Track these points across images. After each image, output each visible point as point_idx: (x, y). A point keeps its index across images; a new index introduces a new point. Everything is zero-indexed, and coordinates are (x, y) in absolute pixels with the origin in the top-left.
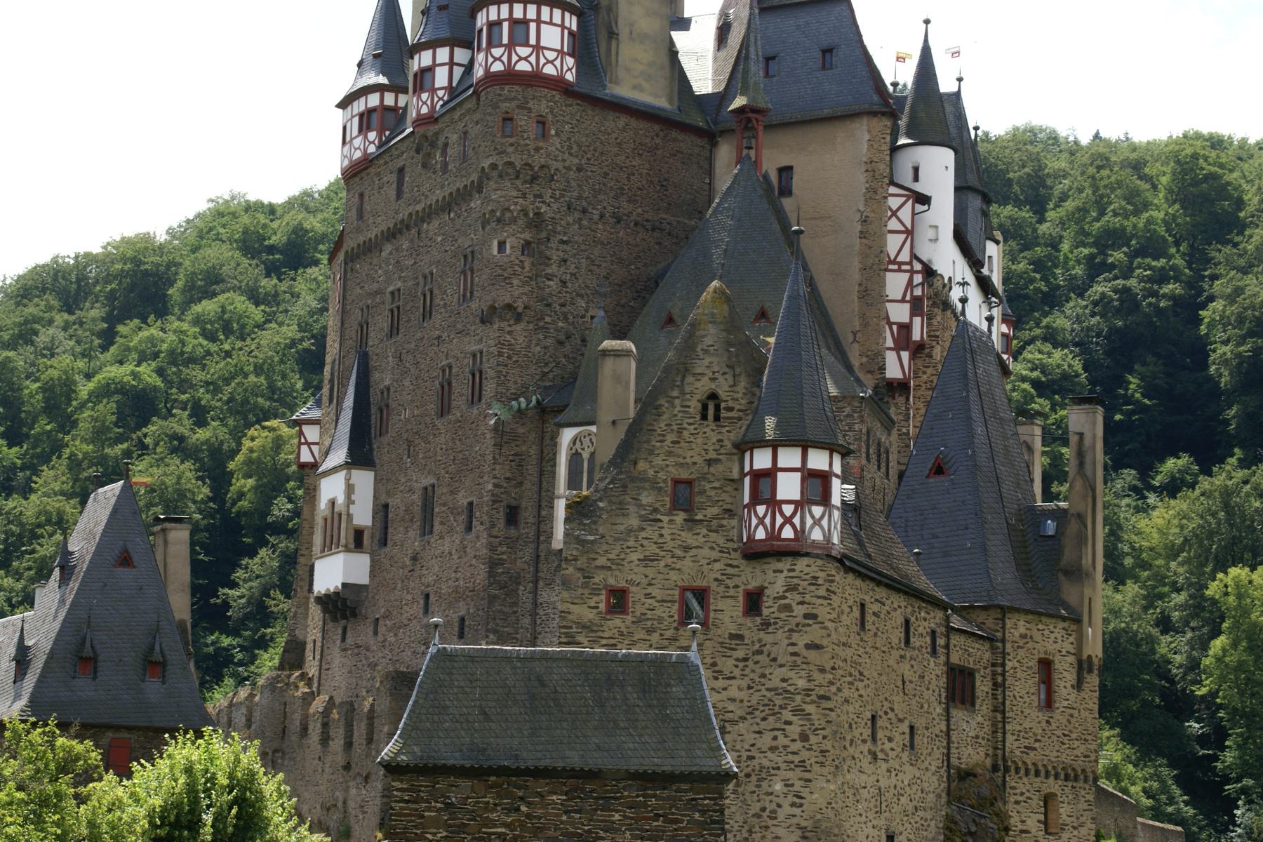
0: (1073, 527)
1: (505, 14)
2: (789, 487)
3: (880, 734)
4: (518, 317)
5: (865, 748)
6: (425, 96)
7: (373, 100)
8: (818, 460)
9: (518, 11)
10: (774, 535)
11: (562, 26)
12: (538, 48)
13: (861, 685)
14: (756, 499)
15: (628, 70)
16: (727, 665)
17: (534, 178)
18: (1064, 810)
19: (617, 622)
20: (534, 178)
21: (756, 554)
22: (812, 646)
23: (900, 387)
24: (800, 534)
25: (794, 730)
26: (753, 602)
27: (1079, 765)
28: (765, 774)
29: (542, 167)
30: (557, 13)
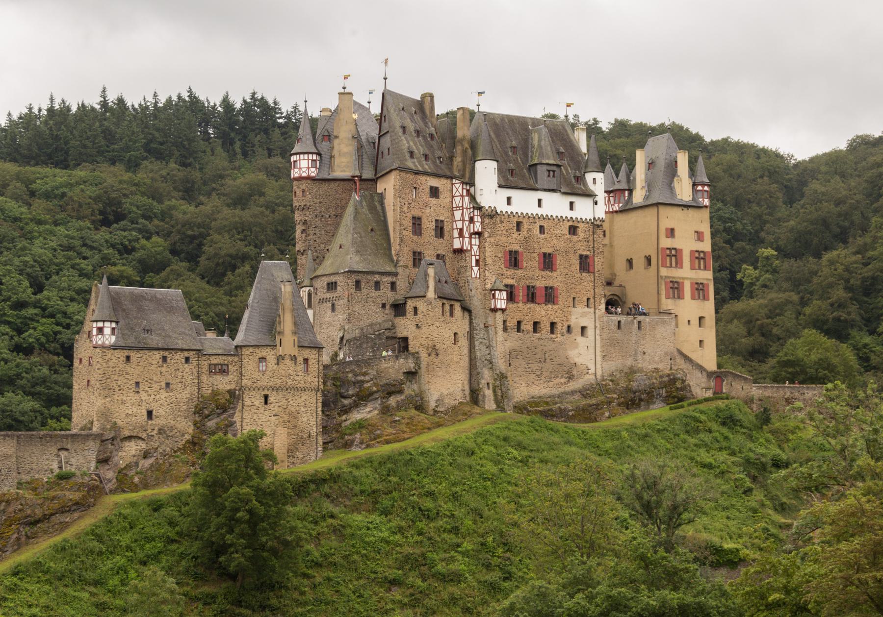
0: (278, 319)
2: (95, 332)
3: (141, 386)
4: (302, 254)
5: (131, 391)
8: (100, 324)
11: (308, 159)
12: (300, 168)
13: (127, 376)
15: (338, 166)
17: (303, 209)
18: (271, 399)
20: (303, 209)
22: (98, 369)
27: (277, 386)
29: (305, 205)
30: (306, 156)
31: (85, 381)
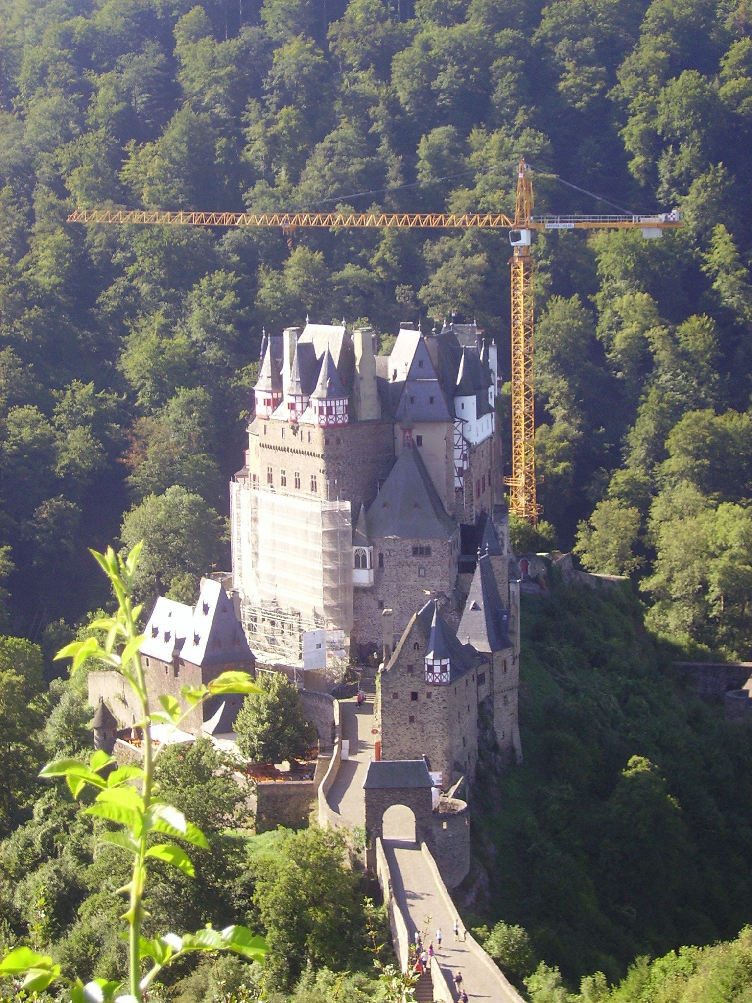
0: (511, 619)
1: (324, 405)
2: (437, 669)
6: (293, 412)
7: (269, 396)
8: (444, 662)
9: (329, 405)
10: (434, 681)
12: (336, 415)
14: (429, 672)
16: (423, 710)
18: (509, 699)
19: (396, 701)
21: (427, 683)
23: (461, 489)
24: (440, 681)
25: (441, 727)
26: (429, 695)
28: (433, 737)
31: (407, 717)
